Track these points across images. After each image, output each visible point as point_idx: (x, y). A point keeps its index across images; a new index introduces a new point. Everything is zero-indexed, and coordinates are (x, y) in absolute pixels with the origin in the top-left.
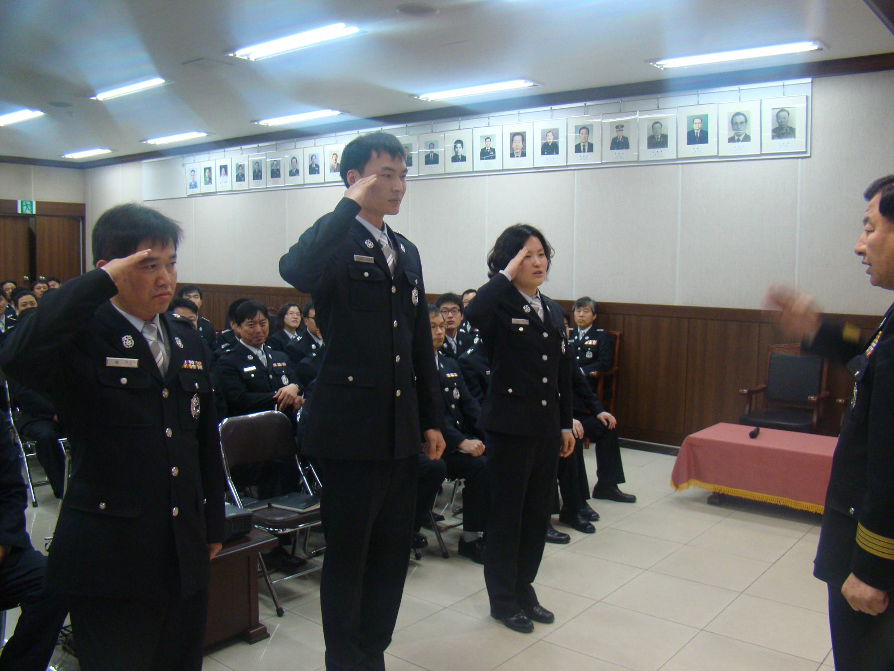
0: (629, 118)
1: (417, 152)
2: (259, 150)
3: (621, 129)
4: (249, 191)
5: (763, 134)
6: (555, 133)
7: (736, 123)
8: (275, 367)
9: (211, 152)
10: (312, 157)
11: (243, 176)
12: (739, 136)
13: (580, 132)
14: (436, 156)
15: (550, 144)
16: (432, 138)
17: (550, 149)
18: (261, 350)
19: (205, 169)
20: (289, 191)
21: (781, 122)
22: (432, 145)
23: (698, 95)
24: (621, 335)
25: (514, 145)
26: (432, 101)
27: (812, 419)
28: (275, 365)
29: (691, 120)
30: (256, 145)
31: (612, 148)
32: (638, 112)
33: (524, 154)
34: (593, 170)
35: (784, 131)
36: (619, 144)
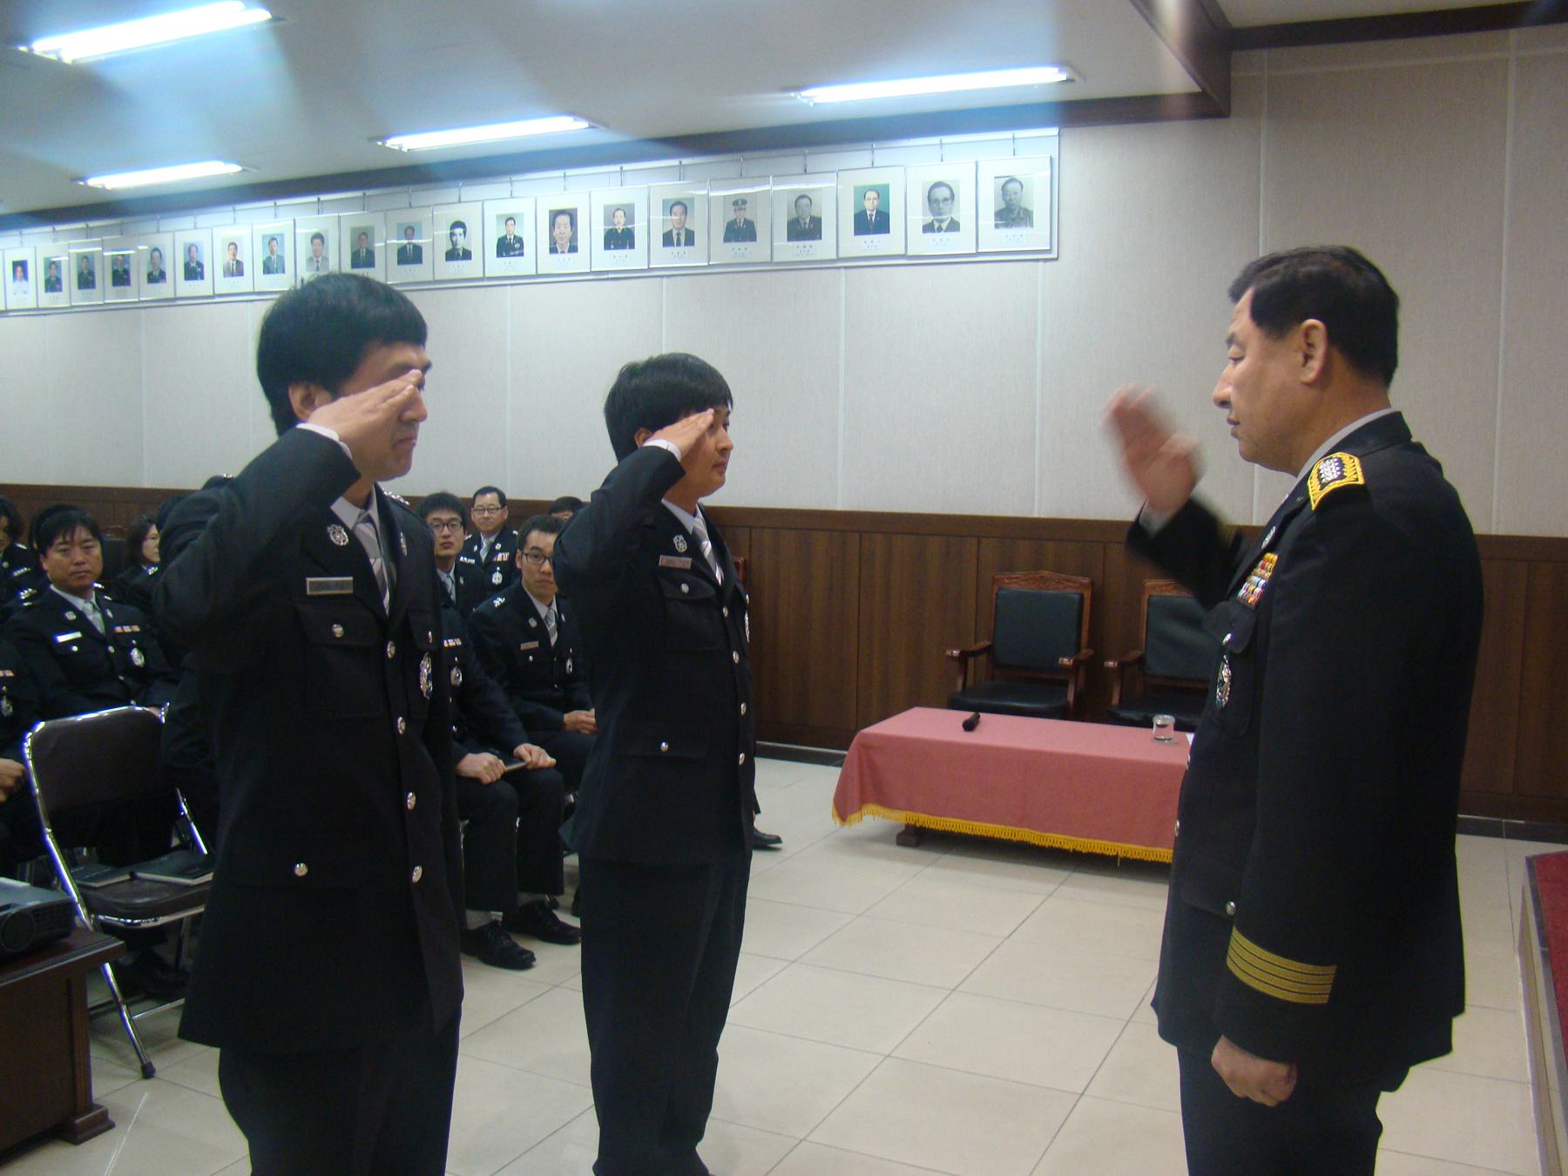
0: (757, 189)
1: (383, 244)
2: (88, 233)
3: (743, 207)
4: (70, 310)
5: (980, 223)
6: (629, 212)
7: (936, 201)
8: (120, 633)
10: (190, 249)
11: (59, 281)
12: (941, 221)
13: (671, 209)
15: (620, 231)
16: (408, 217)
17: (619, 239)
18: (91, 603)
20: (148, 310)
21: (1010, 200)
22: (409, 231)
24: (745, 562)
25: (557, 232)
26: (409, 150)
27: (1066, 696)
28: (118, 629)
29: (861, 193)
30: (81, 225)
31: (727, 239)
32: (771, 178)
33: (573, 249)
34: (694, 278)
35: (1015, 215)
36: (741, 231)
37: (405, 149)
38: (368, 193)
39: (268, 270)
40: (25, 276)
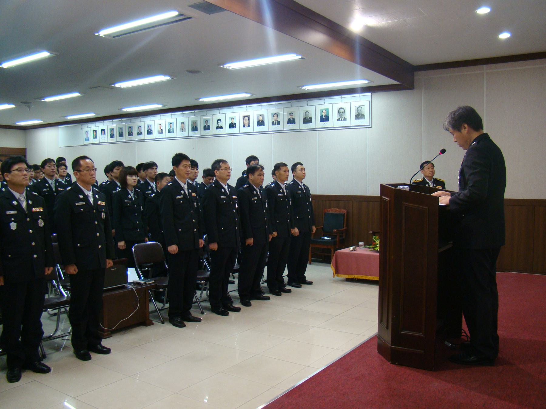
2: (121, 122)
6: (263, 116)
7: (340, 113)
9: (97, 122)
10: (149, 126)
11: (113, 135)
12: (342, 118)
14: (209, 126)
17: (261, 123)
19: (94, 131)
23: (324, 99)
25: (245, 121)
29: (322, 111)
30: (120, 120)
31: (288, 123)
33: (249, 126)
36: (291, 121)
37: (205, 101)
38: (196, 111)
39: (169, 132)
40: (105, 133)
